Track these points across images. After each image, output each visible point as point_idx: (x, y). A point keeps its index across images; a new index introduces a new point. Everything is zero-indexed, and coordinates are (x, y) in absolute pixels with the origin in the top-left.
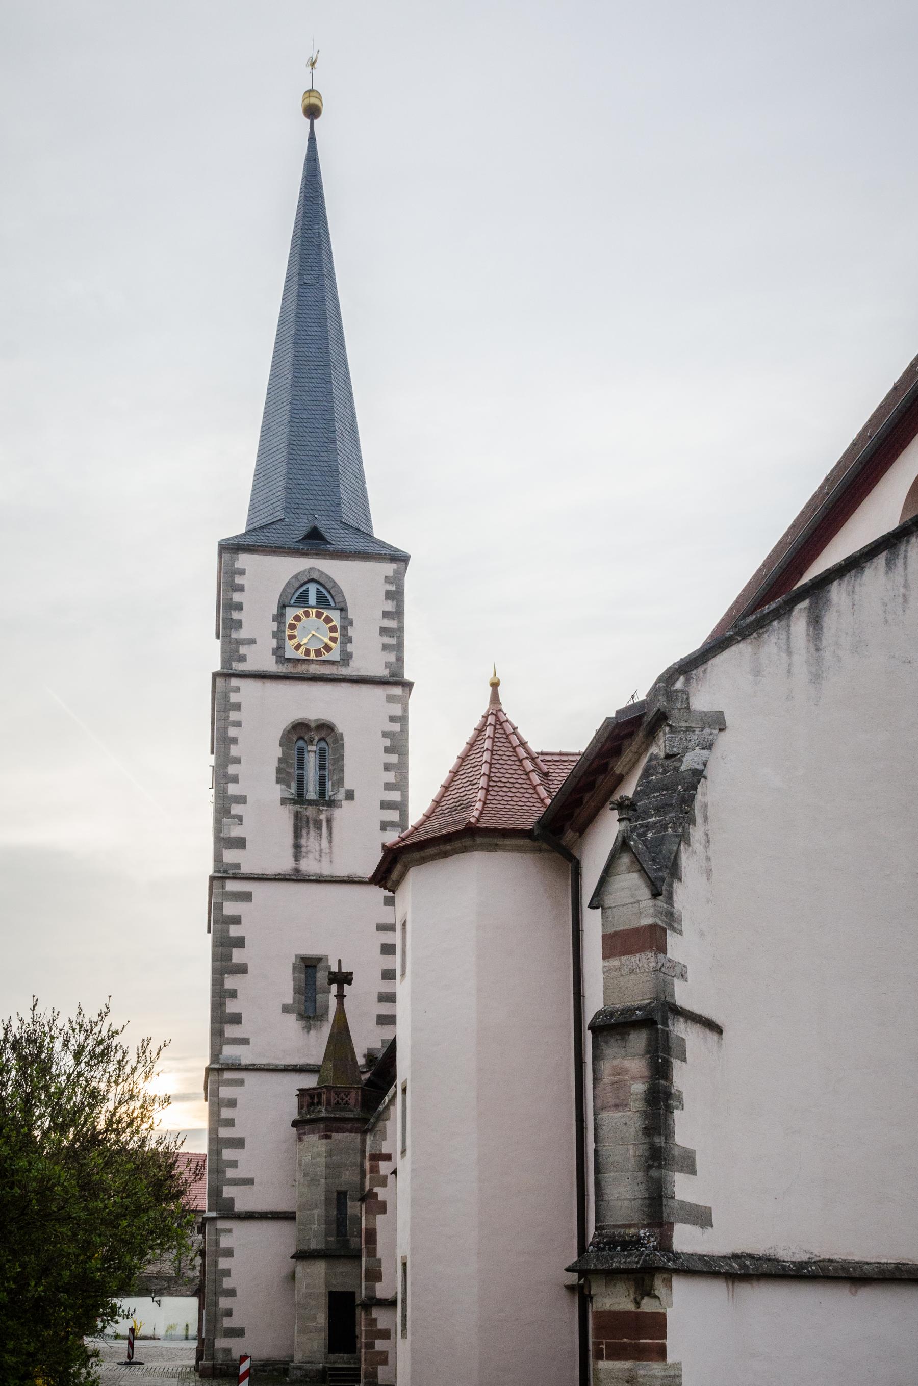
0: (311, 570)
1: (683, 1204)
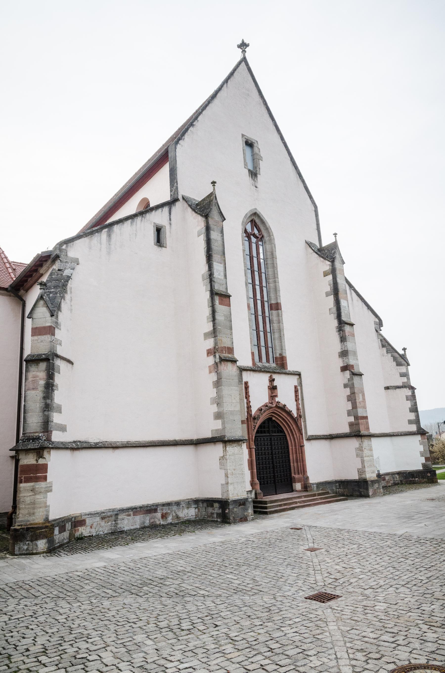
1: (56, 424)
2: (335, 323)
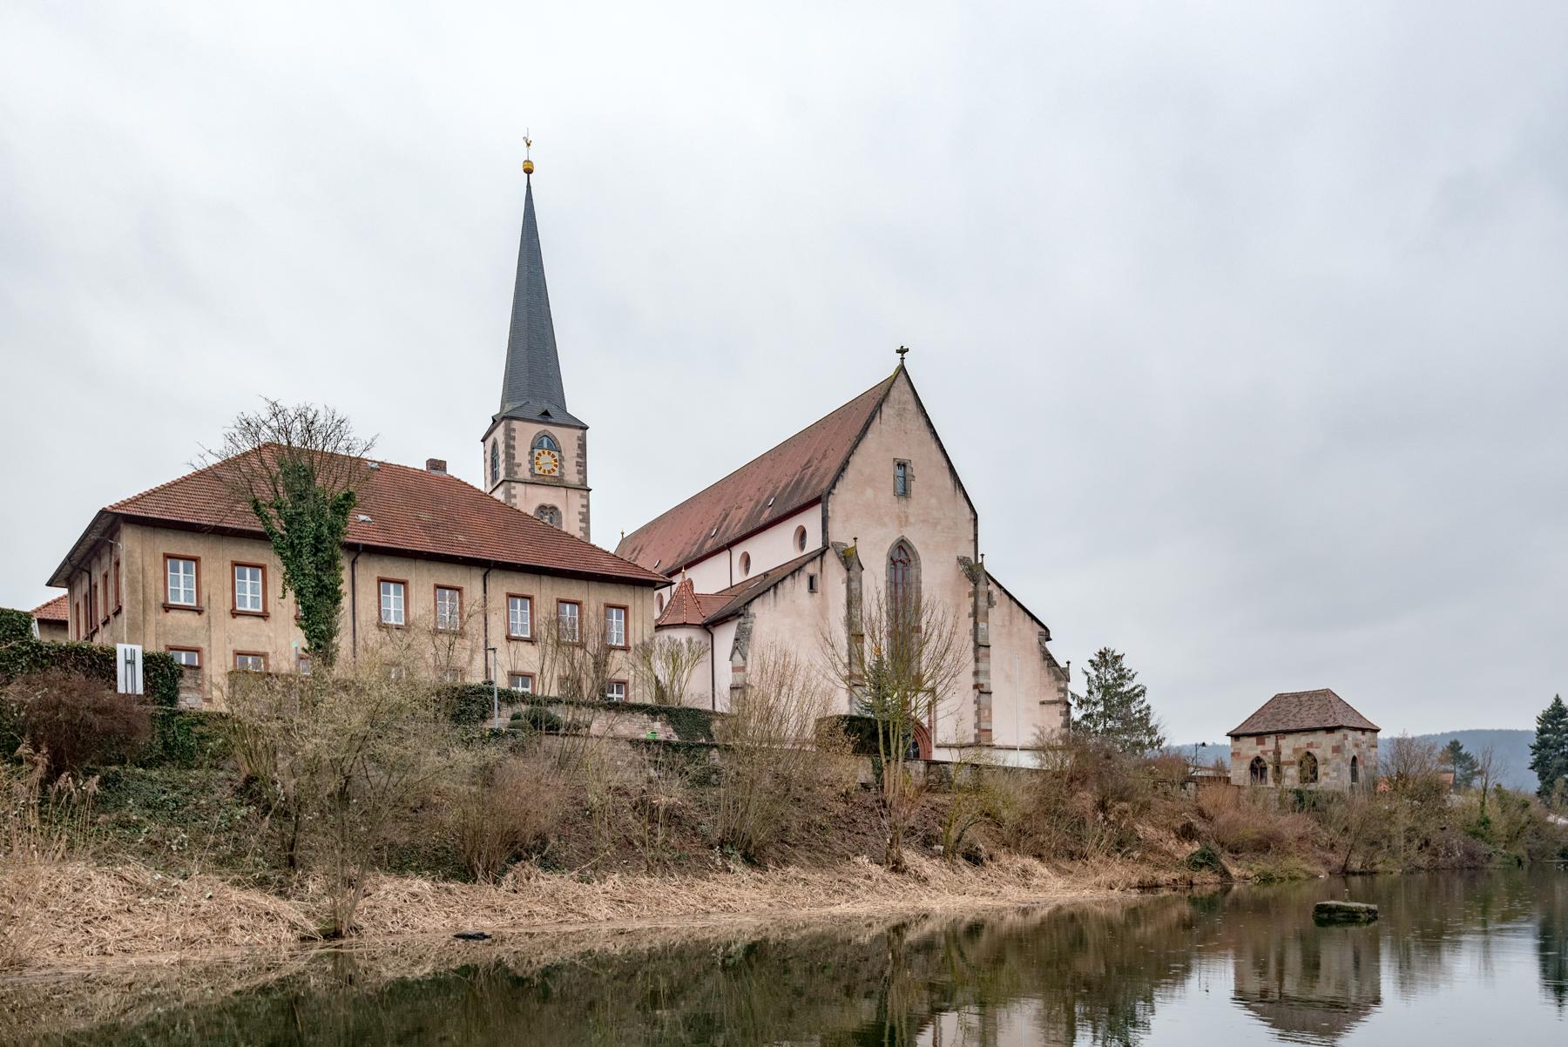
0: (545, 430)
2: (972, 644)
